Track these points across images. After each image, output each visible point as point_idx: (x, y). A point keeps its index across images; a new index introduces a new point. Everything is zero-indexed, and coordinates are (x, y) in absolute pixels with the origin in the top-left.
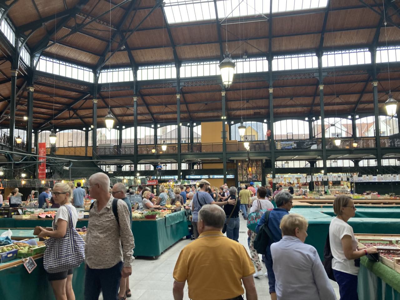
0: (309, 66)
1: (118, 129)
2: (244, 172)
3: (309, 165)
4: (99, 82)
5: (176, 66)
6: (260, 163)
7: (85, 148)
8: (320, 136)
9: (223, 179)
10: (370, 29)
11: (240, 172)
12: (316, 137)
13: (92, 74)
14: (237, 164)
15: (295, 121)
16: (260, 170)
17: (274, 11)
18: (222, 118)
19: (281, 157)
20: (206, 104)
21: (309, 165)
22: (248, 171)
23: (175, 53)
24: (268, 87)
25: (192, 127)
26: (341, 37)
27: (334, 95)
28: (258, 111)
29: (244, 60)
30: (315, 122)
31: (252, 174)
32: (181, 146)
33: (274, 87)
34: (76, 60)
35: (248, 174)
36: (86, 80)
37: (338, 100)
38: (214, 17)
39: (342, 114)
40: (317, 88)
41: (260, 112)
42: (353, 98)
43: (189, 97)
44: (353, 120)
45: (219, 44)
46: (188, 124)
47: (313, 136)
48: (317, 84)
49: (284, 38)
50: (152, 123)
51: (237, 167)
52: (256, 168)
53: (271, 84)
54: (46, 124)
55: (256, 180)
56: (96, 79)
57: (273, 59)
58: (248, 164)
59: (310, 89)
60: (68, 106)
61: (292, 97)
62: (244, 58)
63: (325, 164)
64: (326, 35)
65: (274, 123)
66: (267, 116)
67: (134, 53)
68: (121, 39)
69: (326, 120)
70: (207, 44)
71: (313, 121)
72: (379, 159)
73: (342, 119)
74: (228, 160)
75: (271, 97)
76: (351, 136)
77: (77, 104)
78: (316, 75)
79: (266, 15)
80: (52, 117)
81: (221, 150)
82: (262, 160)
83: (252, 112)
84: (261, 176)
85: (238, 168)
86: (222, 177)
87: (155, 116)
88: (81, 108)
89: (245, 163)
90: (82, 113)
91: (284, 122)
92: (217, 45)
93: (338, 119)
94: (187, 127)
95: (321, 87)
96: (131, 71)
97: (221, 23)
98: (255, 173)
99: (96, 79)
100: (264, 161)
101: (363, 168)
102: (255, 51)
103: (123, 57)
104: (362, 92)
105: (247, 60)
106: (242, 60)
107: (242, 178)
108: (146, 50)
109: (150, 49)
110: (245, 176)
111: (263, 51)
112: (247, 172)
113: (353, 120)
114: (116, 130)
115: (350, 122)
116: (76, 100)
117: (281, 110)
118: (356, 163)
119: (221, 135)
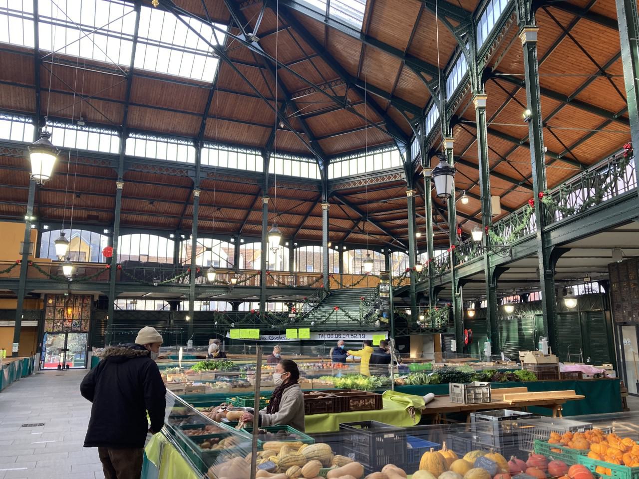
0: (182, 159)
2: (59, 316)
3: (168, 307)
6: (88, 301)
11: (49, 315)
12: (183, 265)
14: (45, 301)
15: (154, 238)
16: (87, 313)
18: (26, 218)
19: (125, 294)
21: (169, 306)
22: (65, 314)
24: (115, 179)
26: (228, 128)
29: (79, 128)
30: (184, 242)
31: (72, 319)
33: (125, 180)
35: (64, 320)
37: (218, 214)
38: (30, 44)
40: (191, 193)
41: (98, 216)
42: (238, 214)
44: (237, 244)
48: (191, 188)
49: (149, 110)
51: (45, 306)
52: (80, 310)
53: (121, 175)
55: (79, 329)
57: (129, 137)
58: (68, 301)
59: (180, 192)
61: (152, 199)
62: (79, 125)
63: (191, 306)
64: (209, 122)
65: (120, 237)
66: (110, 224)
69: (198, 240)
70: (11, 86)
71: (182, 240)
72: (262, 302)
74: (28, 294)
75: (119, 196)
76: (231, 267)
78: (191, 174)
81: (16, 273)
82: (93, 296)
83: (84, 213)
84: (88, 323)
85: (48, 309)
86: (13, 323)
89: (62, 300)
91: (136, 237)
93: (216, 242)
95: (197, 193)
98: (78, 318)
100: (96, 298)
101: (243, 314)
102: (99, 117)
105: (84, 129)
106: (75, 127)
110: (58, 322)
111: (113, 120)
112: (63, 316)
113: (237, 244)
115: (232, 247)
117: (134, 217)
118: (235, 306)
119: (20, 248)
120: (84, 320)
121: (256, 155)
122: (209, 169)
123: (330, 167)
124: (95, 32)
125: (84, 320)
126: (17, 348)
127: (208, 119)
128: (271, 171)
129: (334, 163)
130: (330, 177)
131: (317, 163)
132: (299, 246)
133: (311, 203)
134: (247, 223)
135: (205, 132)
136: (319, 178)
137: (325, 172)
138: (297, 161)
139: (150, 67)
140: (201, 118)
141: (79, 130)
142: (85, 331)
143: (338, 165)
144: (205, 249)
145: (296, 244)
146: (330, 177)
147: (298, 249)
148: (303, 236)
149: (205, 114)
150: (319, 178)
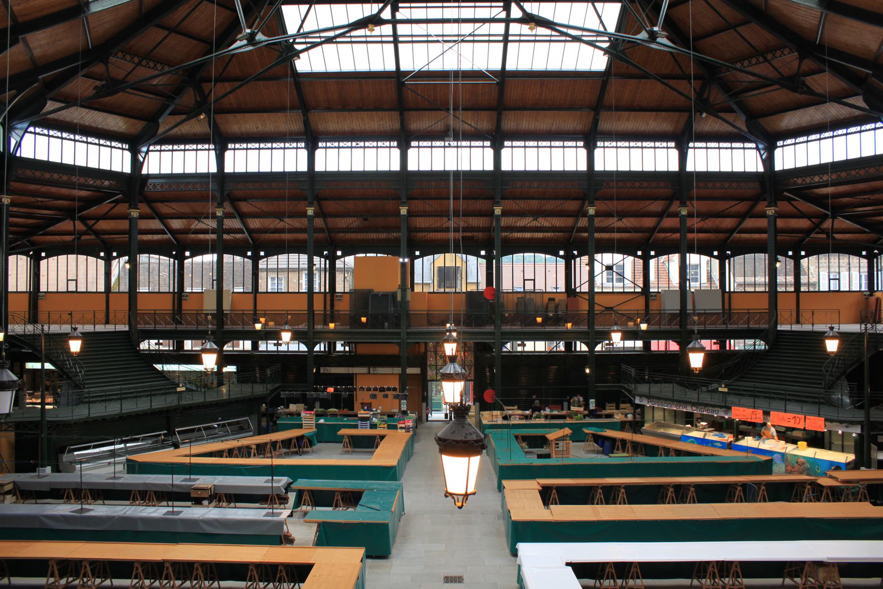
1: (175, 257)
5: (306, 147)
7: (105, 294)
8: (585, 288)
9: (398, 377)
10: (678, 114)
12: (578, 290)
13: (128, 155)
17: (510, 67)
20: (366, 220)
23: (306, 123)
25: (332, 259)
27: (613, 216)
28: (470, 234)
30: (578, 260)
34: (97, 128)
36: (116, 168)
38: (391, 67)
39: (626, 248)
43: (331, 206)
45: (398, 112)
46: (325, 253)
47: (573, 287)
49: (525, 112)
52: (462, 355)
54: (20, 242)
56: (136, 164)
60: (69, 213)
64: (603, 114)
66: (488, 245)
68: (199, 99)
71: (574, 257)
73: (625, 256)
76: (639, 290)
77: (94, 210)
79: (493, 73)
80: (34, 230)
84: (473, 369)
85: (429, 353)
86: (398, 370)
87: (255, 235)
88: (98, 218)
90: (103, 225)
91: (518, 257)
92: (396, 115)
93: (618, 257)
94: (323, 260)
96: (213, 154)
97: (407, 80)
103: (199, 124)
104: (660, 215)
107: (435, 373)
108: (247, 115)
109: (255, 115)
114: (172, 260)
116: (88, 203)
120: (468, 366)
121: (667, 148)
122: (607, 175)
123: (778, 152)
125: (468, 366)
126: (405, 406)
127: (602, 113)
128: (690, 168)
129: (783, 146)
130: (778, 167)
131: (757, 148)
133: (750, 203)
134: (659, 232)
135: (598, 128)
136: (761, 169)
137: (769, 162)
138: (726, 148)
139: (524, 65)
140: (593, 113)
141: (447, 147)
142: (469, 378)
143: (789, 150)
144: (604, 268)
146: (778, 167)
147: (732, 259)
148: (739, 241)
149: (598, 106)
150: (761, 169)
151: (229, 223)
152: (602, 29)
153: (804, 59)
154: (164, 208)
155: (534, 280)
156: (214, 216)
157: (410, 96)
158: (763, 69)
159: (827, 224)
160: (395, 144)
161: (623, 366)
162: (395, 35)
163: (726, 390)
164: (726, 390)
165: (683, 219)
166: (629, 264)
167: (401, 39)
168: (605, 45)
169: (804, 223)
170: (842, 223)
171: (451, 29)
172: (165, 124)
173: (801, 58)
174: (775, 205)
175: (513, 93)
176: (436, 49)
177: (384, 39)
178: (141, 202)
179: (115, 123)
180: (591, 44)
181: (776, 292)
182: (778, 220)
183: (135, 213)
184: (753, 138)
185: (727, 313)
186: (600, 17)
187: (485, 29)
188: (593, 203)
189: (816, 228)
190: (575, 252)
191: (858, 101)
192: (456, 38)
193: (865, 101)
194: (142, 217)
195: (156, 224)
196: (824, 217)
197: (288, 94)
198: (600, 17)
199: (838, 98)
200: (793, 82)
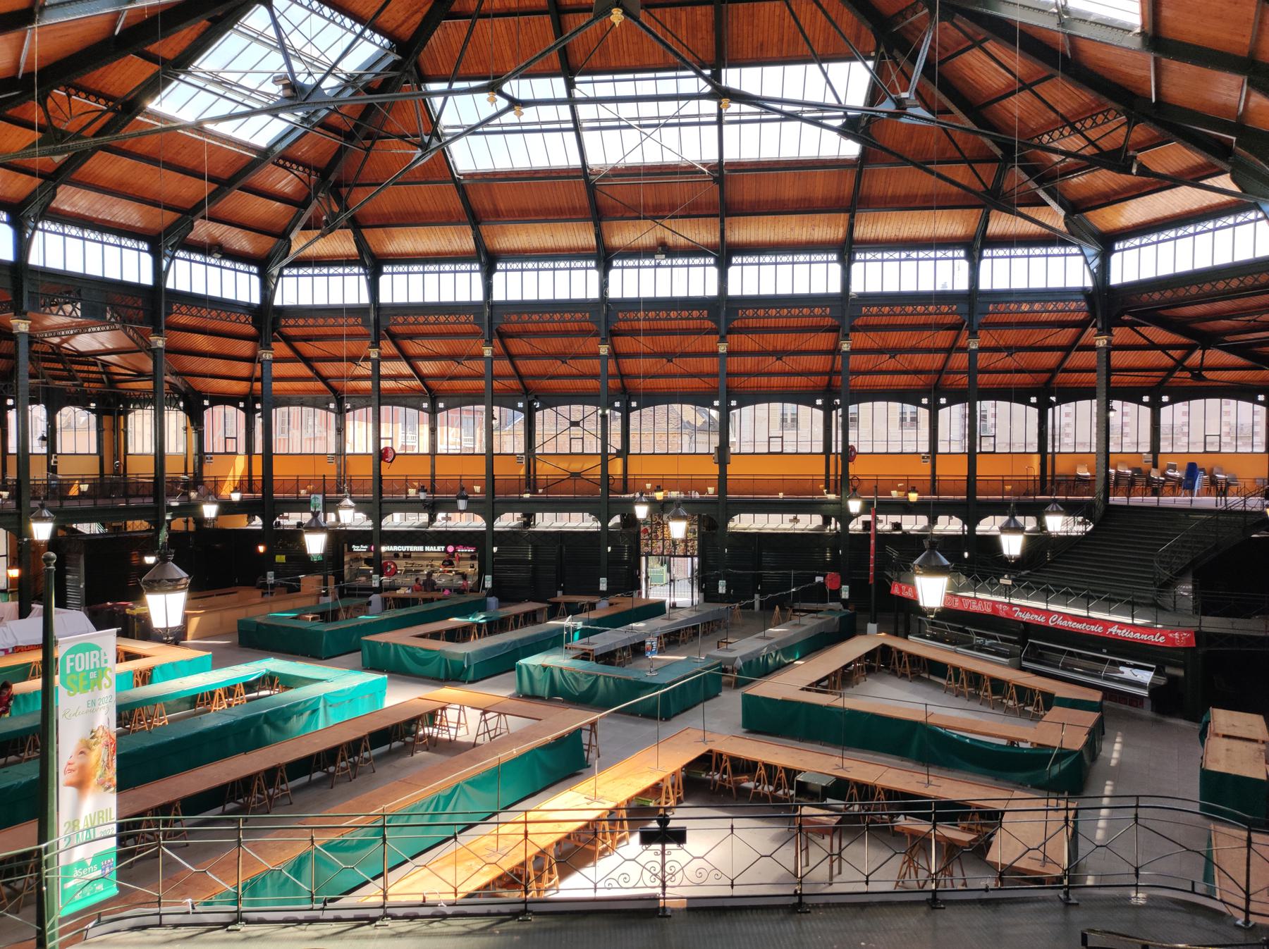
4: (277, 302)
13: (256, 281)
23: (478, 239)
32: (493, 480)
38: (576, 162)
50: (423, 399)
67: (367, 233)
99: (267, 291)
103: (343, 243)
104: (949, 351)
123: (1115, 259)
124: (665, 125)
128: (984, 285)
130: (1115, 279)
132: (1059, 402)
136: (1089, 283)
143: (1131, 256)
145: (1053, 399)
146: (1115, 279)
147: (1057, 408)
150: (1089, 283)
151: (387, 368)
152: (831, 100)
153: (1136, 123)
154: (308, 349)
155: (782, 437)
156: (367, 359)
157: (603, 200)
158: (1074, 143)
159: (1196, 357)
160: (593, 264)
161: (888, 548)
162: (575, 119)
163: (1010, 582)
164: (1010, 582)
165: (973, 354)
166: (810, 419)
167: (585, 125)
168: (838, 123)
169: (1155, 358)
170: (1216, 356)
171: (648, 109)
172: (299, 242)
173: (1130, 124)
174: (1109, 333)
175: (747, 190)
176: (632, 136)
177: (564, 126)
178: (276, 340)
179: (240, 240)
180: (814, 122)
181: (534, 455)
182: (1114, 354)
183: (268, 356)
184: (1075, 240)
185: (531, 482)
186: (828, 81)
187: (691, 107)
188: (848, 335)
189: (1179, 365)
190: (181, 404)
191: (1224, 181)
192: (656, 122)
193: (1234, 180)
194: (277, 360)
195: (300, 369)
196: (1190, 349)
197: (455, 203)
198: (828, 81)
199: (1193, 178)
200: (1116, 160)
